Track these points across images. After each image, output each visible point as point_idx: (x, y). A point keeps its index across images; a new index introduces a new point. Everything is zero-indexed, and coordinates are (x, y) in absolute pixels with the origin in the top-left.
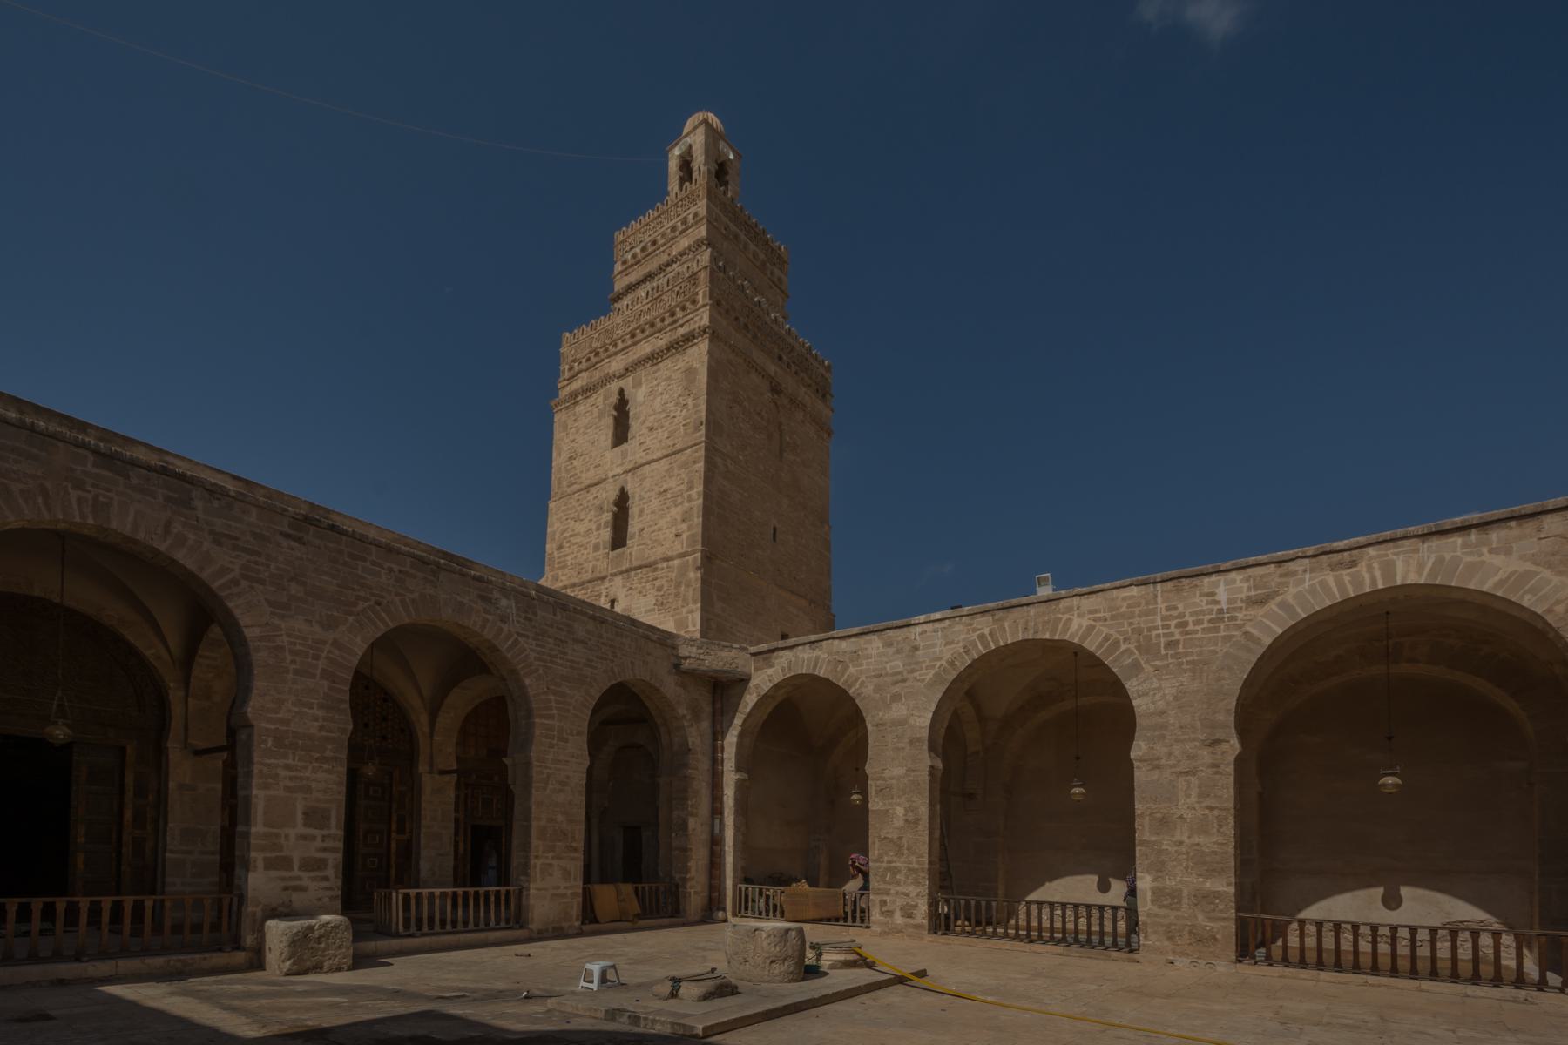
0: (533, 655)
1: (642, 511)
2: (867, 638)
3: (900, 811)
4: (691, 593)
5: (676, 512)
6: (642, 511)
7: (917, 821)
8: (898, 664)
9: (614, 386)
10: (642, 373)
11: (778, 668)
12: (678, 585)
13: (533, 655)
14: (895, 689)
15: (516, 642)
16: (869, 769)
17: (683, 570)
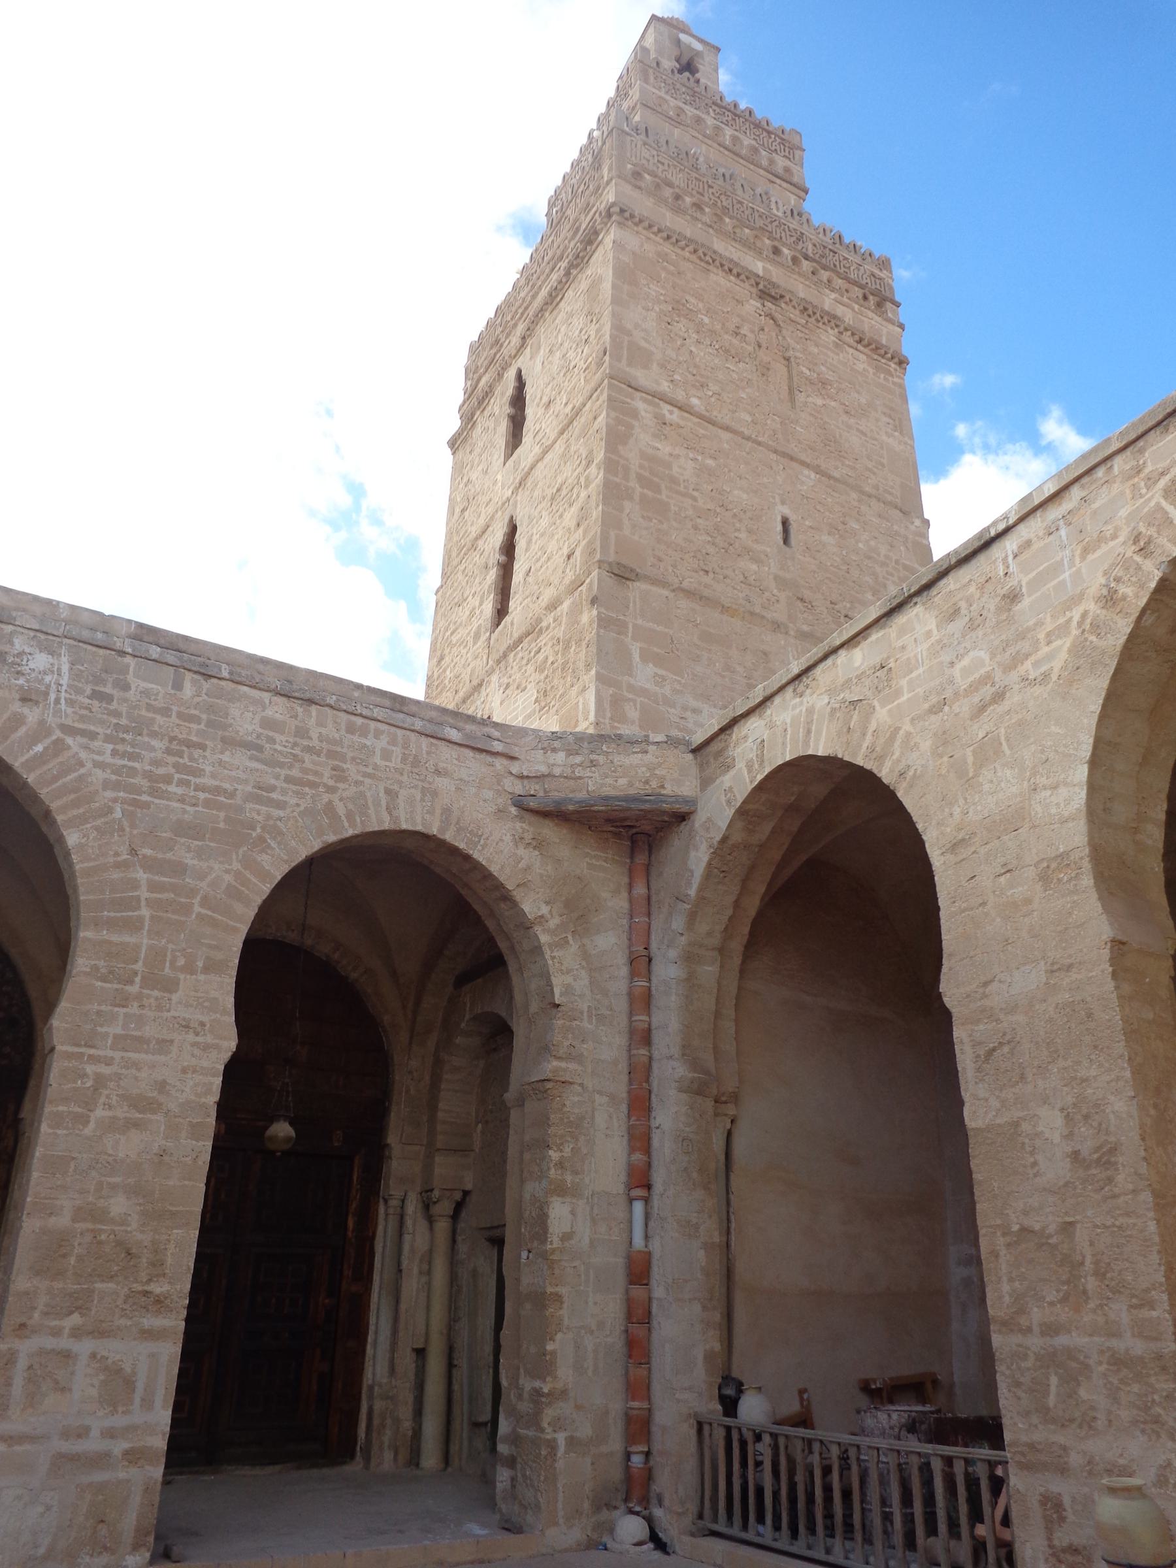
0: (100, 775)
1: (529, 542)
2: (901, 619)
3: (1051, 1123)
4: (582, 655)
5: (570, 516)
6: (529, 542)
7: (1106, 1157)
8: (978, 658)
9: (511, 374)
10: (541, 330)
11: (741, 765)
12: (567, 647)
13: (100, 775)
14: (979, 731)
15: (59, 747)
16: (953, 988)
17: (575, 611)
